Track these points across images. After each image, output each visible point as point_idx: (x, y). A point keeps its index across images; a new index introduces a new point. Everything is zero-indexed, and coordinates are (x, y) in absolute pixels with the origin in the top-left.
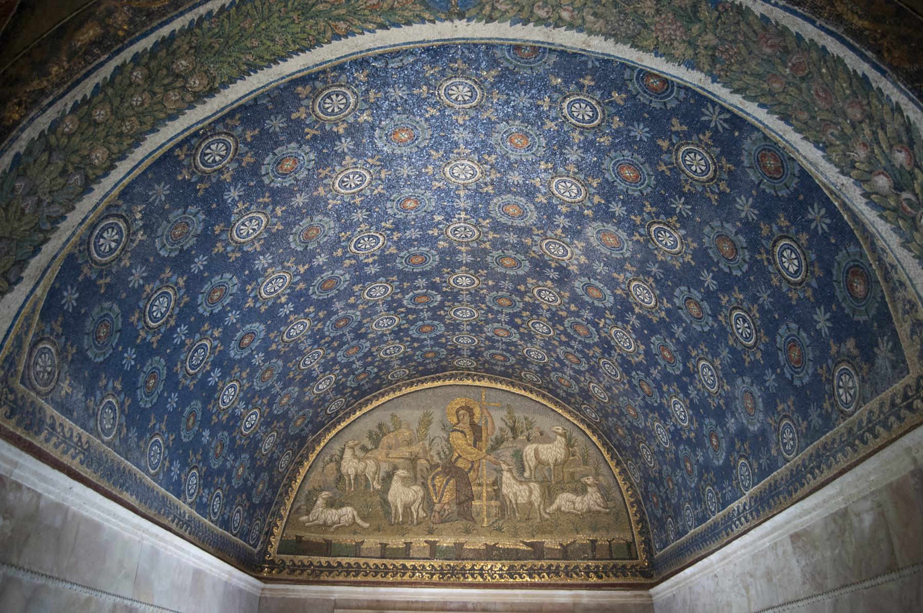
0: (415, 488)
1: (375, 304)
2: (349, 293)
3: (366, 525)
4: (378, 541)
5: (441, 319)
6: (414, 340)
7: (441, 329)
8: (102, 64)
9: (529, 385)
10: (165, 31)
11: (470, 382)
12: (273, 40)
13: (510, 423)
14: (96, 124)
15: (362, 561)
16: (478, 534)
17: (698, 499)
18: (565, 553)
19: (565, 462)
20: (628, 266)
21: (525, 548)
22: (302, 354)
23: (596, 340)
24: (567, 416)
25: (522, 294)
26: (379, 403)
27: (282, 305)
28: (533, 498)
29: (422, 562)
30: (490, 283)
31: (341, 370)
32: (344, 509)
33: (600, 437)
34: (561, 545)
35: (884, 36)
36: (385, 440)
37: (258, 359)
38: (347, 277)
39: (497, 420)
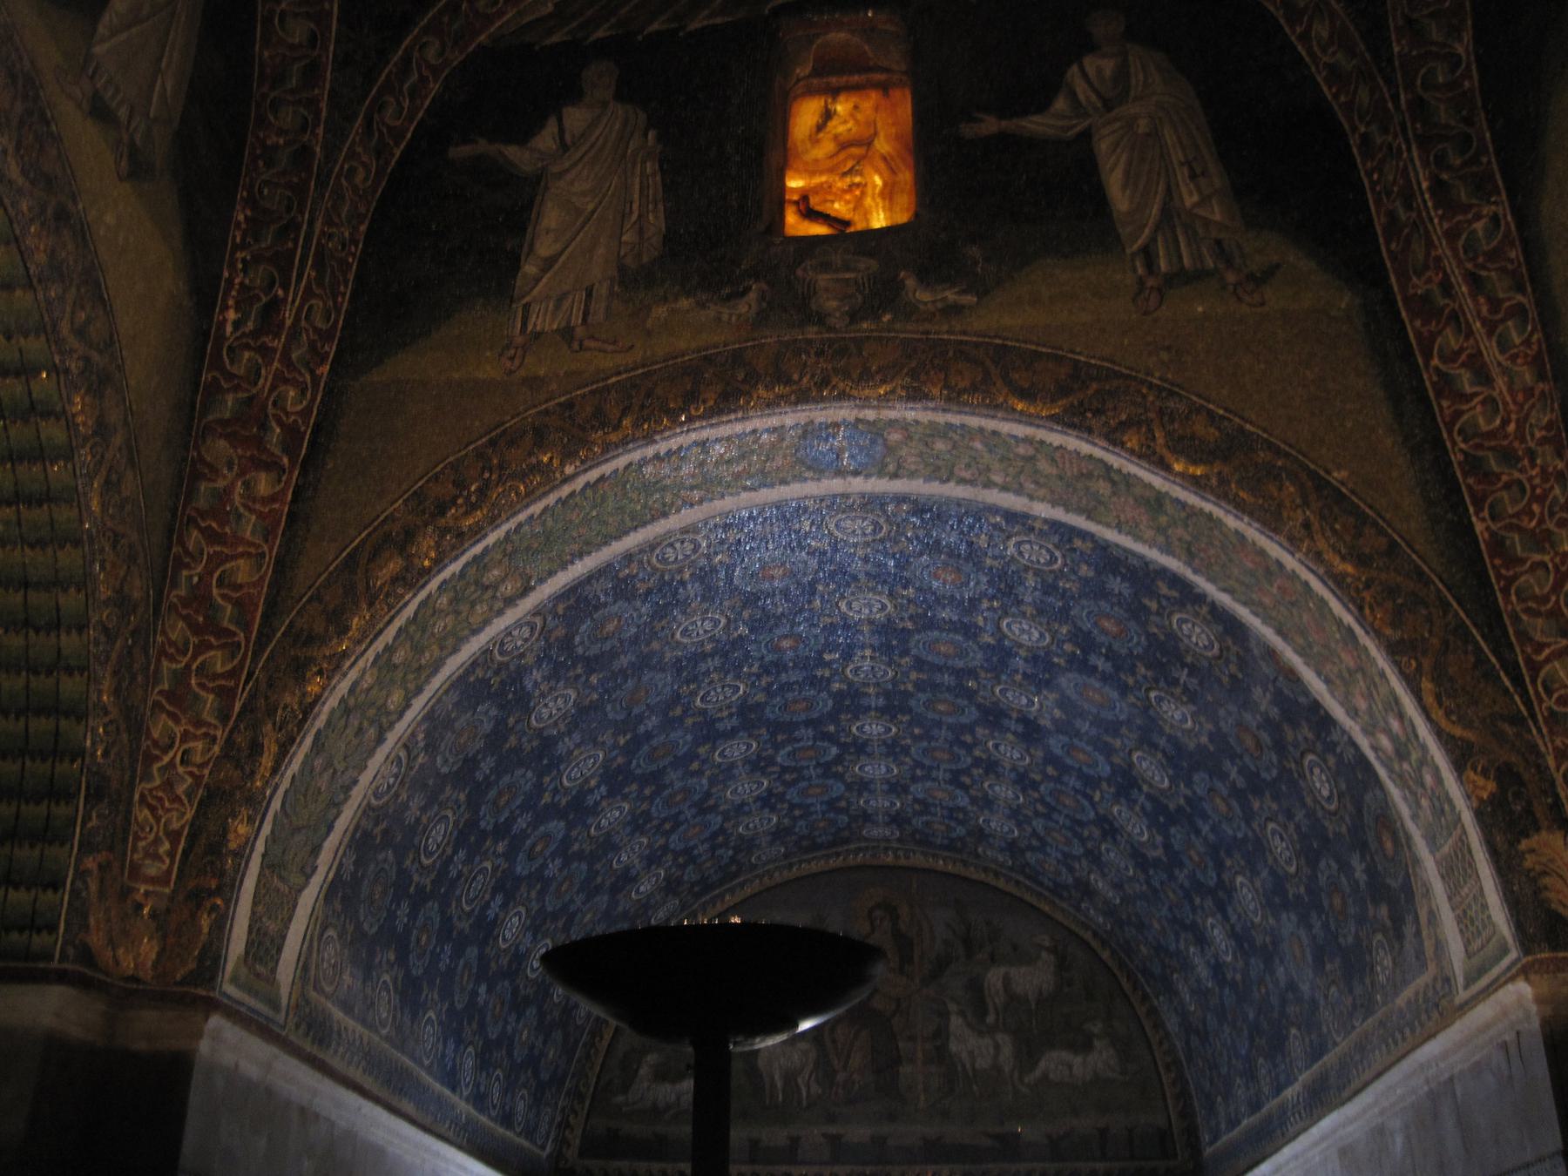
1: (732, 766)
2: (692, 756)
5: (839, 777)
6: (792, 807)
7: (838, 789)
8: (406, 604)
10: (478, 549)
12: (605, 523)
14: (396, 667)
17: (1251, 1075)
20: (1124, 730)
22: (616, 848)
23: (1092, 815)
25: (969, 748)
27: (591, 791)
30: (917, 731)
31: (675, 859)
35: (1367, 586)
37: (553, 868)
38: (689, 738)
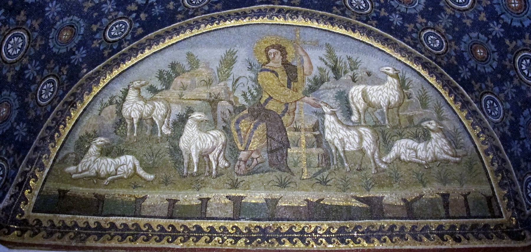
0: (215, 133)
3: (150, 177)
4: (165, 196)
9: (354, 21)
11: (281, 21)
13: (331, 63)
15: (142, 221)
16: (297, 188)
18: (410, 209)
19: (400, 105)
21: (358, 204)
24: (398, 57)
26: (173, 41)
28: (365, 144)
29: (222, 223)
32: (123, 158)
33: (440, 77)
34: (404, 200)
36: (178, 81)
39: (314, 61)
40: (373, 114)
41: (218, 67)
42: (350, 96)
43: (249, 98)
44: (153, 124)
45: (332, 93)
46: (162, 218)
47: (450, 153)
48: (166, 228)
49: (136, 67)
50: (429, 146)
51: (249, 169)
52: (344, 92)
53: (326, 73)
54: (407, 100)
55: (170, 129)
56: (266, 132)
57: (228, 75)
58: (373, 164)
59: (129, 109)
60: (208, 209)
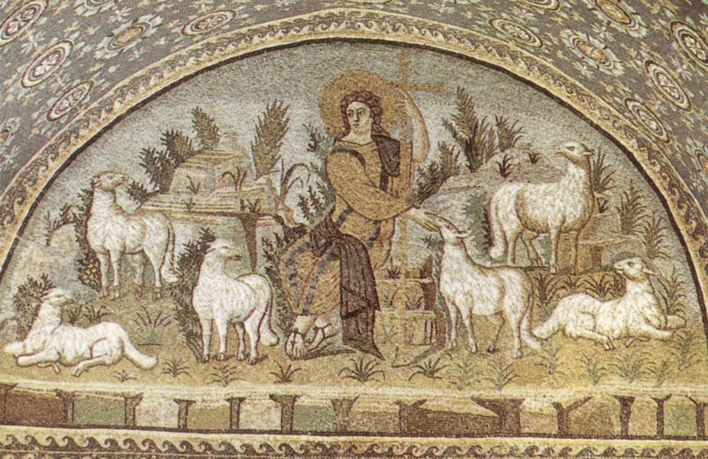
3: (147, 361)
21: (481, 410)
32: (100, 329)
40: (531, 245)
41: (254, 142)
42: (493, 206)
43: (312, 210)
44: (146, 262)
45: (460, 199)
46: (171, 430)
47: (655, 322)
48: (177, 446)
49: (101, 140)
50: (619, 307)
51: (309, 348)
52: (483, 197)
53: (454, 156)
54: (599, 215)
55: (175, 273)
56: (339, 279)
57: (274, 160)
58: (516, 340)
59: (100, 233)
60: (241, 416)
